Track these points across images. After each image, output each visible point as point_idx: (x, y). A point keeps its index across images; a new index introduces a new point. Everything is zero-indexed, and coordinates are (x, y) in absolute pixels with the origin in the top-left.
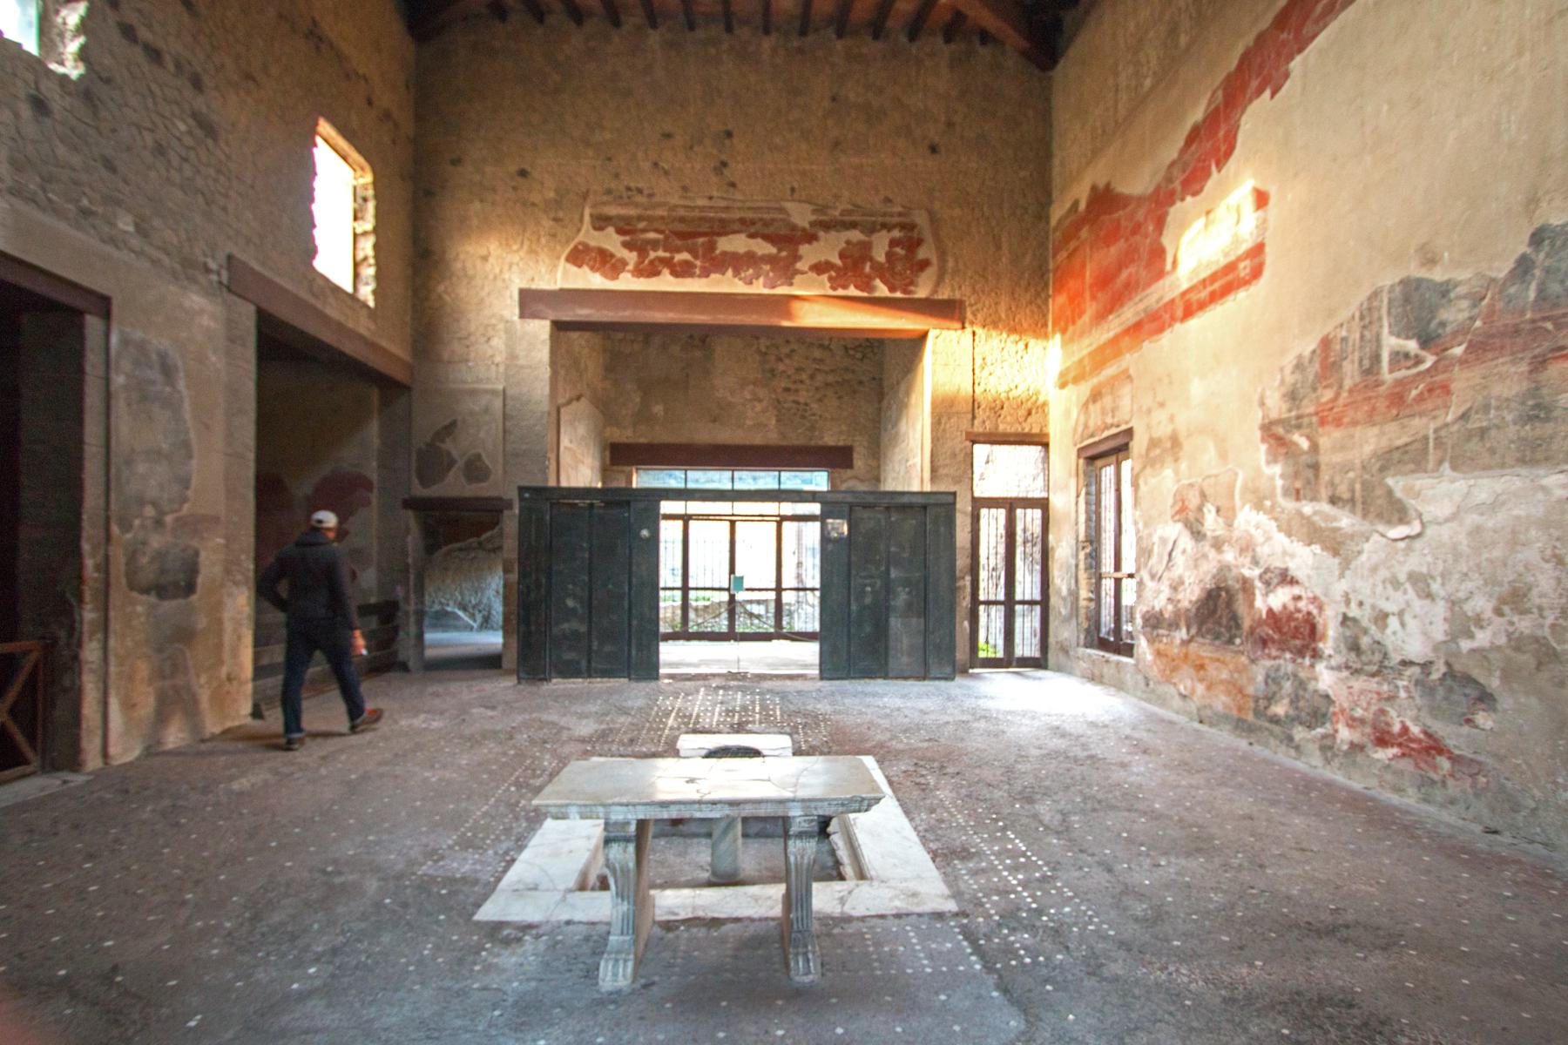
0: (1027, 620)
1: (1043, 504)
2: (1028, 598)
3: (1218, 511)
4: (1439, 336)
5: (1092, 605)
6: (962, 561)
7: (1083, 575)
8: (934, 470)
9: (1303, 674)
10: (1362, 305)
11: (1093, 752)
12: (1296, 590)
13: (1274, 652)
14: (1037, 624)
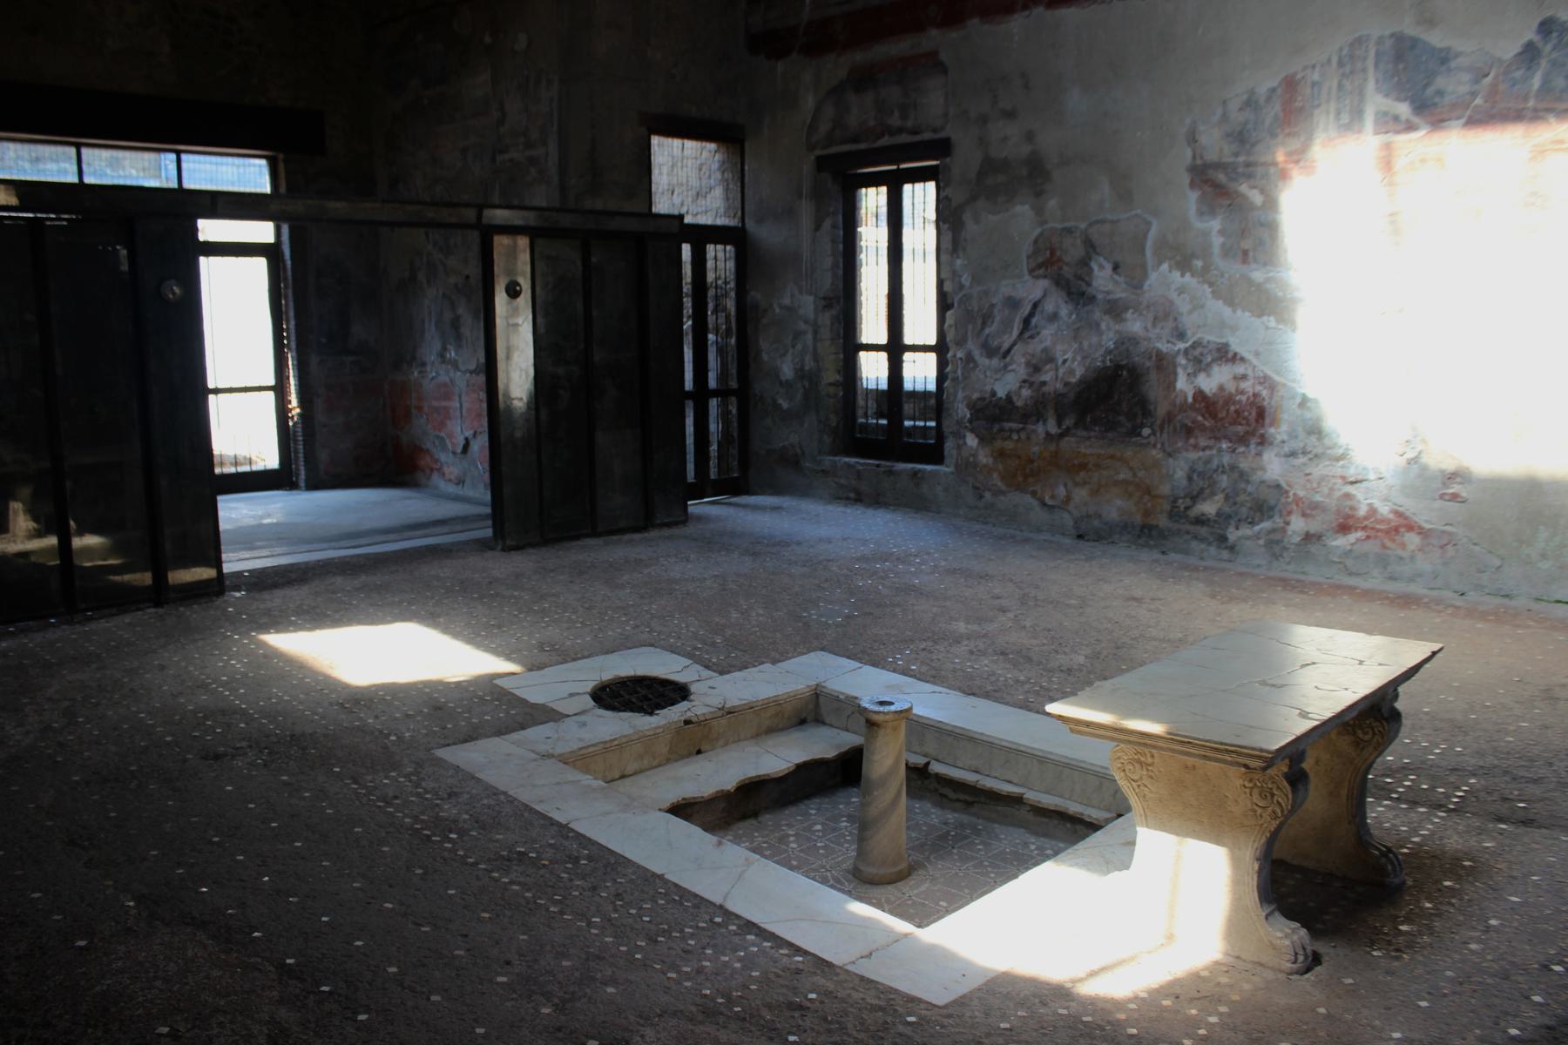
3: (1116, 268)
4: (1435, 104)
9: (1244, 465)
10: (1341, 49)
12: (1240, 369)
13: (1203, 442)
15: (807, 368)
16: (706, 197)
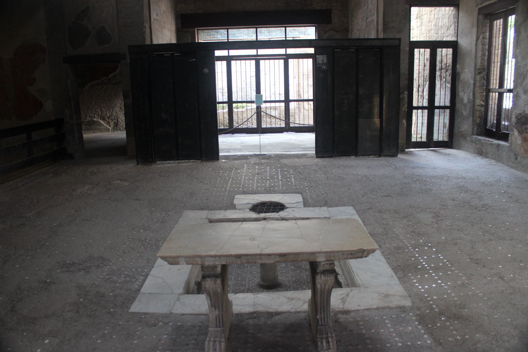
0: (442, 117)
1: (453, 45)
2: (442, 104)
5: (483, 109)
6: (403, 82)
7: (478, 90)
8: (385, 24)
11: (486, 202)
14: (447, 121)
15: (471, 99)
16: (449, 29)
